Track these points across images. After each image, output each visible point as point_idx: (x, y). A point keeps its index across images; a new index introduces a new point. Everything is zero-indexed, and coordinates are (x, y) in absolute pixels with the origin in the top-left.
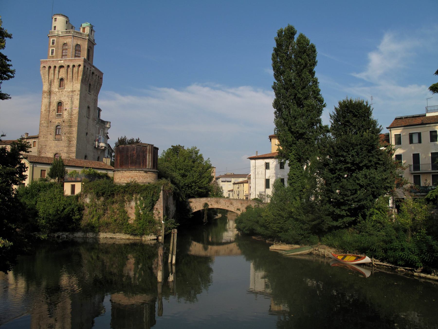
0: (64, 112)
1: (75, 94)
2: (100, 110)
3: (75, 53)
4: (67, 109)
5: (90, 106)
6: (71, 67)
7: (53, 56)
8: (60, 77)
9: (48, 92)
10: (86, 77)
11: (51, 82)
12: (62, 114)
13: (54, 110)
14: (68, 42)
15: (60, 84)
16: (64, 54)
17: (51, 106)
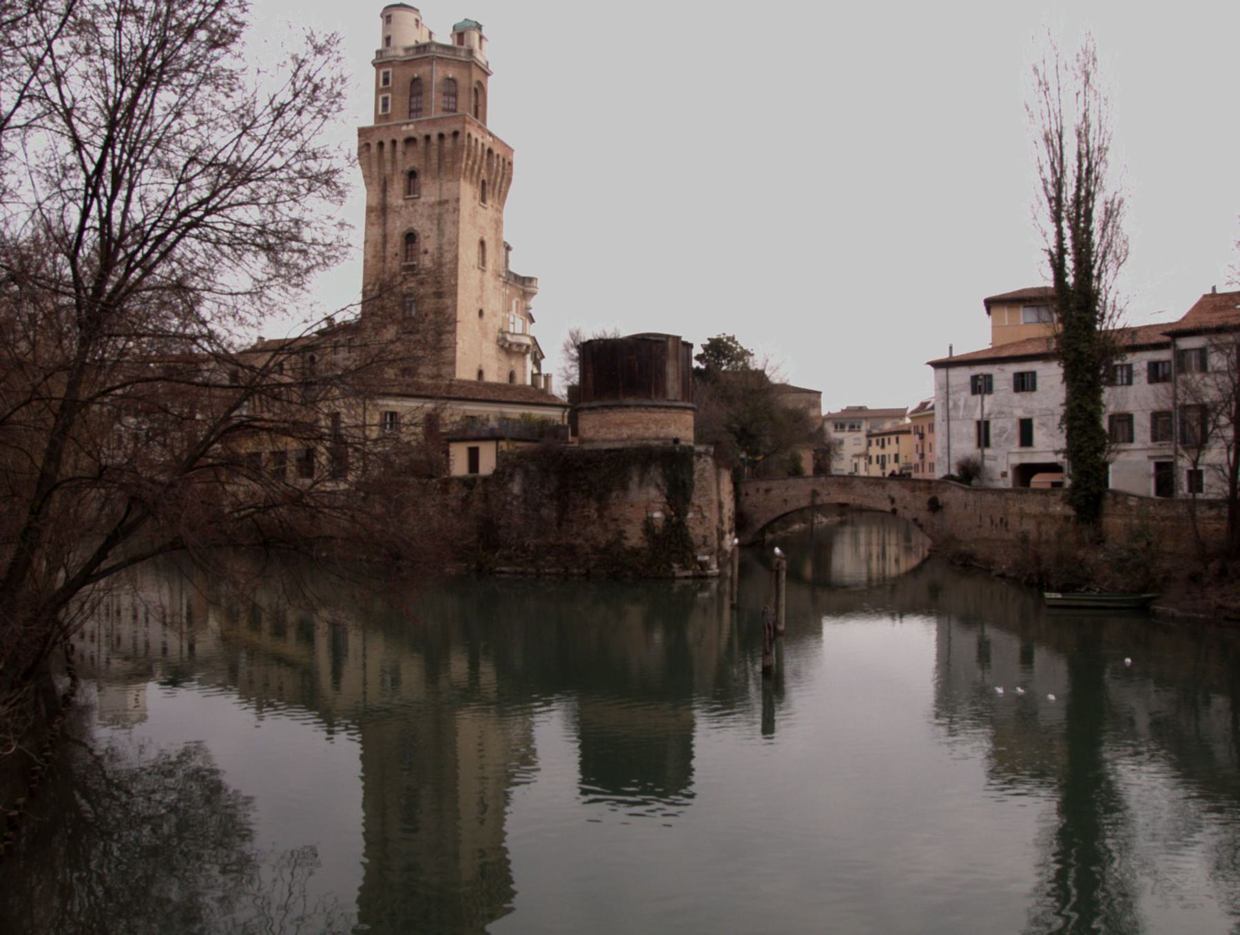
0: (421, 257)
1: (448, 210)
2: (508, 248)
4: (430, 250)
5: (486, 239)
6: (434, 139)
8: (407, 168)
9: (379, 208)
10: (474, 163)
12: (415, 263)
13: (396, 255)
15: (409, 187)
16: (414, 107)
17: (389, 246)
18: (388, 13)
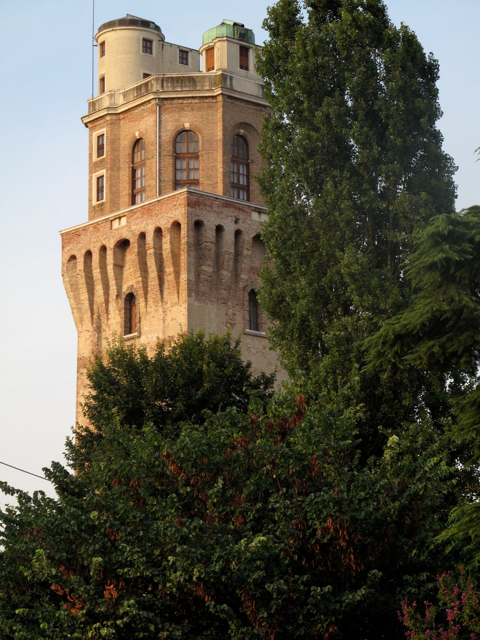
3: (175, 170)
7: (102, 204)
8: (125, 289)
11: (99, 317)
14: (146, 129)
18: (100, 40)
